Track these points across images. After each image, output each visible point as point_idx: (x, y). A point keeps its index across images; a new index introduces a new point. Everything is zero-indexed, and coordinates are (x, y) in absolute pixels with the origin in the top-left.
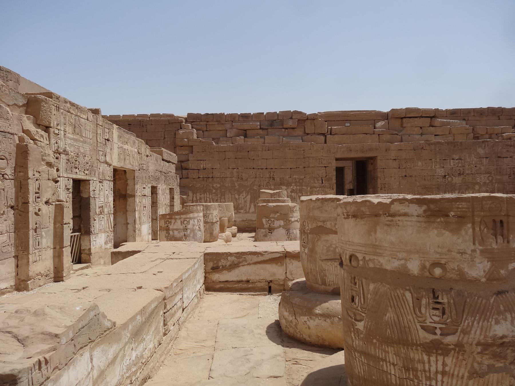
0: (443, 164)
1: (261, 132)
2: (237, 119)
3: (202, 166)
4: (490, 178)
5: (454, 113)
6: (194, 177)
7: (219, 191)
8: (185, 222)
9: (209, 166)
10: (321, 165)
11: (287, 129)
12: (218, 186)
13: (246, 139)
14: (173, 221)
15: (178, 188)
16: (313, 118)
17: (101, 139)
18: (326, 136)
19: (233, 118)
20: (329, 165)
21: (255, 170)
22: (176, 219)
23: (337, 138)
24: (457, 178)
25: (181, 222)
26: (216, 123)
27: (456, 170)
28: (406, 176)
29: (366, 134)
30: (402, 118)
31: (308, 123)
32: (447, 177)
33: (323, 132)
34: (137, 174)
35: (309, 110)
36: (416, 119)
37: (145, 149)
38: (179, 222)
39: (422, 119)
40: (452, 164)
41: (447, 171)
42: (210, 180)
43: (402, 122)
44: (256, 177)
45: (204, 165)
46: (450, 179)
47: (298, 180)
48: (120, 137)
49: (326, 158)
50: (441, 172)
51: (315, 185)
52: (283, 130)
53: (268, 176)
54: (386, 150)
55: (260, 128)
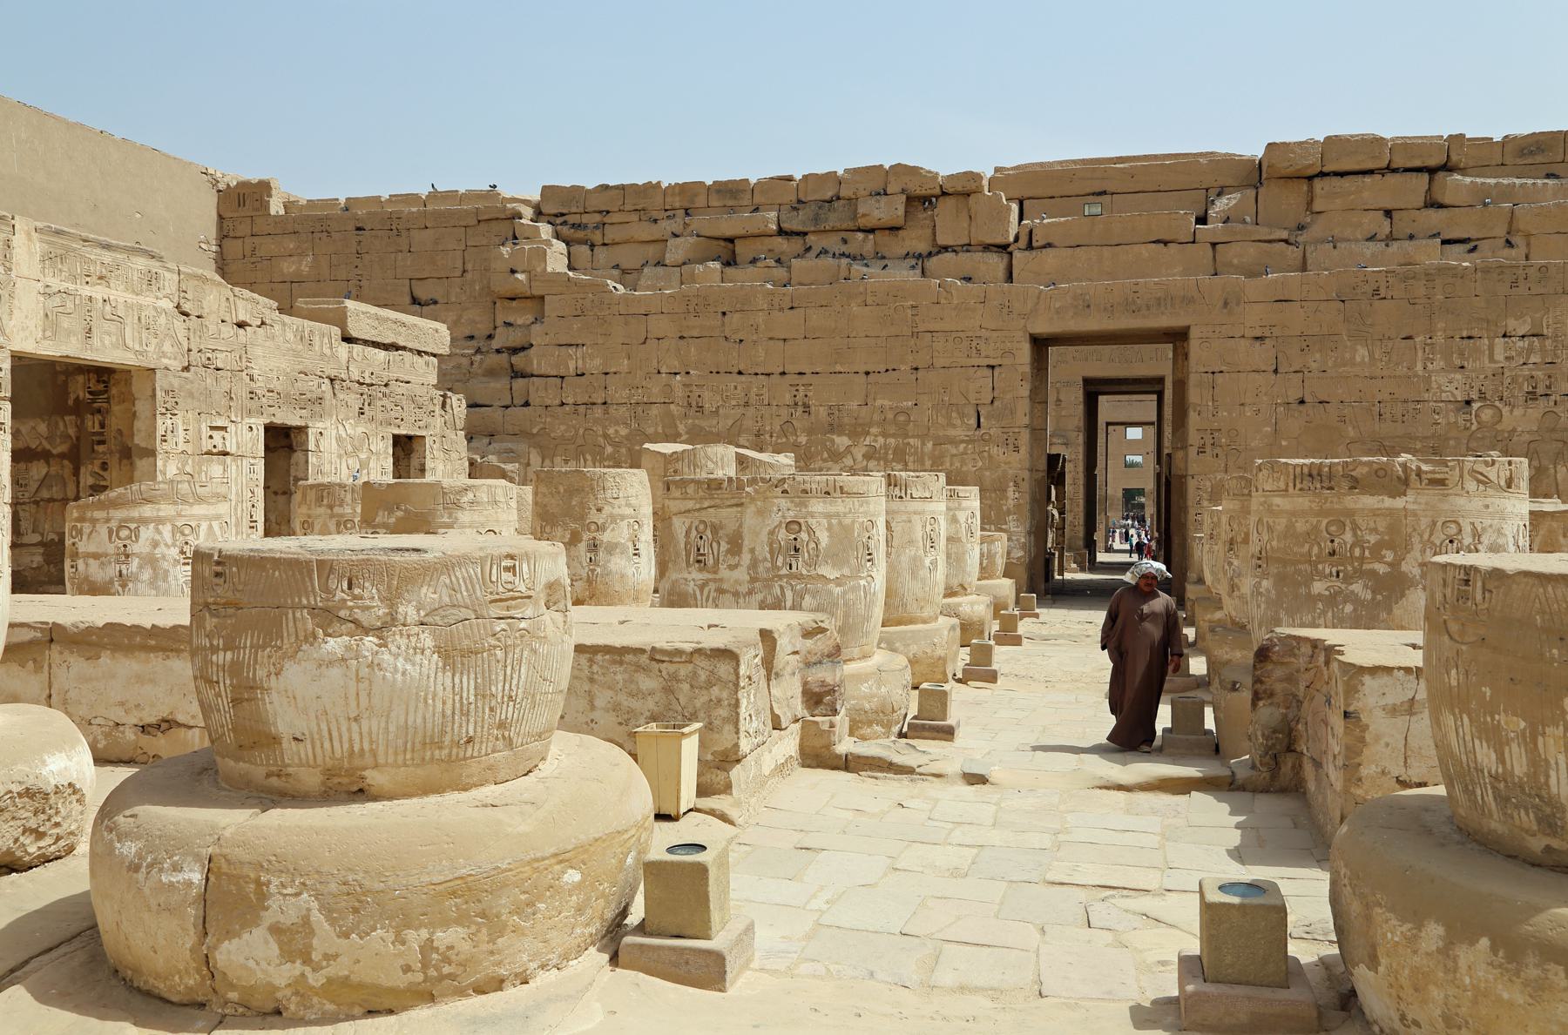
0: (1461, 354)
1: (781, 244)
2: (701, 201)
3: (572, 365)
6: (548, 402)
7: (623, 450)
8: (124, 533)
9: (595, 364)
10: (976, 362)
11: (872, 231)
12: (624, 432)
13: (728, 270)
14: (87, 527)
16: (963, 190)
18: (1011, 254)
20: (1005, 362)
21: (743, 378)
22: (94, 521)
24: (1518, 412)
25: (110, 532)
26: (634, 217)
27: (1514, 380)
28: (1302, 402)
29: (1166, 243)
30: (1310, 178)
31: (946, 207)
32: (1475, 406)
33: (999, 240)
36: (1368, 179)
38: (103, 530)
39: (1391, 179)
40: (1499, 355)
41: (1477, 385)
42: (598, 412)
43: (1311, 190)
44: (747, 404)
45: (580, 362)
46: (1487, 415)
47: (890, 416)
49: (995, 334)
50: (1452, 386)
51: (952, 432)
52: (860, 236)
53: (788, 399)
54: (1226, 304)
55: (781, 232)
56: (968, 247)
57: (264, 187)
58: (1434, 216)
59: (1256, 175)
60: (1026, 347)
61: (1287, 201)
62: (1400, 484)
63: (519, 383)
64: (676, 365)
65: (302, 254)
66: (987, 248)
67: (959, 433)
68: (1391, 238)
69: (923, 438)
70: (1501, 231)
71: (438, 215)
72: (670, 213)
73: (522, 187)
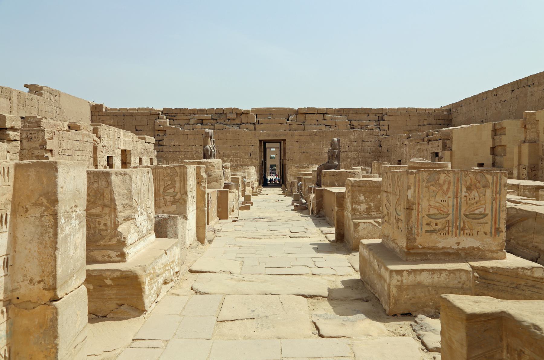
4: (357, 155)
5: (339, 111)
9: (177, 144)
15: (156, 158)
16: (246, 113)
17: (116, 138)
19: (194, 112)
23: (262, 126)
31: (243, 116)
34: (131, 152)
35: (244, 106)
37: (136, 138)
39: (318, 115)
42: (178, 153)
48: (124, 135)
56: (247, 123)
57: (102, 106)
58: (324, 121)
59: (297, 112)
60: (259, 142)
61: (301, 118)
62: (305, 168)
63: (161, 147)
64: (193, 144)
65: (111, 120)
66: (251, 123)
67: (247, 157)
68: (318, 125)
69: (241, 158)
70: (334, 124)
71: (141, 113)
72: (190, 114)
73: (159, 107)
